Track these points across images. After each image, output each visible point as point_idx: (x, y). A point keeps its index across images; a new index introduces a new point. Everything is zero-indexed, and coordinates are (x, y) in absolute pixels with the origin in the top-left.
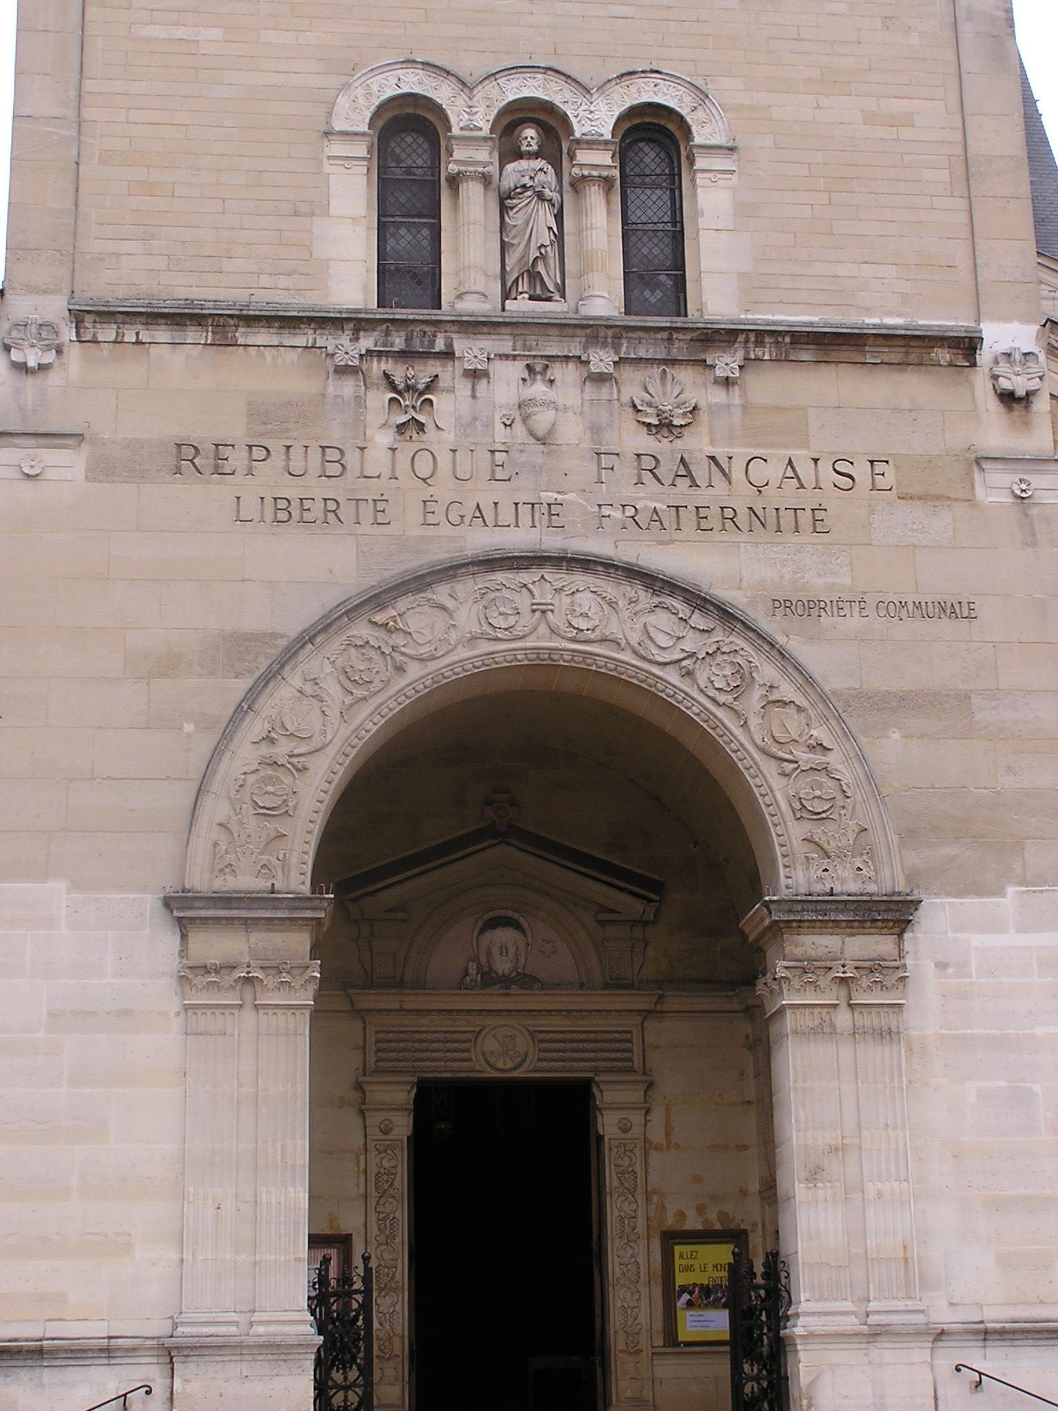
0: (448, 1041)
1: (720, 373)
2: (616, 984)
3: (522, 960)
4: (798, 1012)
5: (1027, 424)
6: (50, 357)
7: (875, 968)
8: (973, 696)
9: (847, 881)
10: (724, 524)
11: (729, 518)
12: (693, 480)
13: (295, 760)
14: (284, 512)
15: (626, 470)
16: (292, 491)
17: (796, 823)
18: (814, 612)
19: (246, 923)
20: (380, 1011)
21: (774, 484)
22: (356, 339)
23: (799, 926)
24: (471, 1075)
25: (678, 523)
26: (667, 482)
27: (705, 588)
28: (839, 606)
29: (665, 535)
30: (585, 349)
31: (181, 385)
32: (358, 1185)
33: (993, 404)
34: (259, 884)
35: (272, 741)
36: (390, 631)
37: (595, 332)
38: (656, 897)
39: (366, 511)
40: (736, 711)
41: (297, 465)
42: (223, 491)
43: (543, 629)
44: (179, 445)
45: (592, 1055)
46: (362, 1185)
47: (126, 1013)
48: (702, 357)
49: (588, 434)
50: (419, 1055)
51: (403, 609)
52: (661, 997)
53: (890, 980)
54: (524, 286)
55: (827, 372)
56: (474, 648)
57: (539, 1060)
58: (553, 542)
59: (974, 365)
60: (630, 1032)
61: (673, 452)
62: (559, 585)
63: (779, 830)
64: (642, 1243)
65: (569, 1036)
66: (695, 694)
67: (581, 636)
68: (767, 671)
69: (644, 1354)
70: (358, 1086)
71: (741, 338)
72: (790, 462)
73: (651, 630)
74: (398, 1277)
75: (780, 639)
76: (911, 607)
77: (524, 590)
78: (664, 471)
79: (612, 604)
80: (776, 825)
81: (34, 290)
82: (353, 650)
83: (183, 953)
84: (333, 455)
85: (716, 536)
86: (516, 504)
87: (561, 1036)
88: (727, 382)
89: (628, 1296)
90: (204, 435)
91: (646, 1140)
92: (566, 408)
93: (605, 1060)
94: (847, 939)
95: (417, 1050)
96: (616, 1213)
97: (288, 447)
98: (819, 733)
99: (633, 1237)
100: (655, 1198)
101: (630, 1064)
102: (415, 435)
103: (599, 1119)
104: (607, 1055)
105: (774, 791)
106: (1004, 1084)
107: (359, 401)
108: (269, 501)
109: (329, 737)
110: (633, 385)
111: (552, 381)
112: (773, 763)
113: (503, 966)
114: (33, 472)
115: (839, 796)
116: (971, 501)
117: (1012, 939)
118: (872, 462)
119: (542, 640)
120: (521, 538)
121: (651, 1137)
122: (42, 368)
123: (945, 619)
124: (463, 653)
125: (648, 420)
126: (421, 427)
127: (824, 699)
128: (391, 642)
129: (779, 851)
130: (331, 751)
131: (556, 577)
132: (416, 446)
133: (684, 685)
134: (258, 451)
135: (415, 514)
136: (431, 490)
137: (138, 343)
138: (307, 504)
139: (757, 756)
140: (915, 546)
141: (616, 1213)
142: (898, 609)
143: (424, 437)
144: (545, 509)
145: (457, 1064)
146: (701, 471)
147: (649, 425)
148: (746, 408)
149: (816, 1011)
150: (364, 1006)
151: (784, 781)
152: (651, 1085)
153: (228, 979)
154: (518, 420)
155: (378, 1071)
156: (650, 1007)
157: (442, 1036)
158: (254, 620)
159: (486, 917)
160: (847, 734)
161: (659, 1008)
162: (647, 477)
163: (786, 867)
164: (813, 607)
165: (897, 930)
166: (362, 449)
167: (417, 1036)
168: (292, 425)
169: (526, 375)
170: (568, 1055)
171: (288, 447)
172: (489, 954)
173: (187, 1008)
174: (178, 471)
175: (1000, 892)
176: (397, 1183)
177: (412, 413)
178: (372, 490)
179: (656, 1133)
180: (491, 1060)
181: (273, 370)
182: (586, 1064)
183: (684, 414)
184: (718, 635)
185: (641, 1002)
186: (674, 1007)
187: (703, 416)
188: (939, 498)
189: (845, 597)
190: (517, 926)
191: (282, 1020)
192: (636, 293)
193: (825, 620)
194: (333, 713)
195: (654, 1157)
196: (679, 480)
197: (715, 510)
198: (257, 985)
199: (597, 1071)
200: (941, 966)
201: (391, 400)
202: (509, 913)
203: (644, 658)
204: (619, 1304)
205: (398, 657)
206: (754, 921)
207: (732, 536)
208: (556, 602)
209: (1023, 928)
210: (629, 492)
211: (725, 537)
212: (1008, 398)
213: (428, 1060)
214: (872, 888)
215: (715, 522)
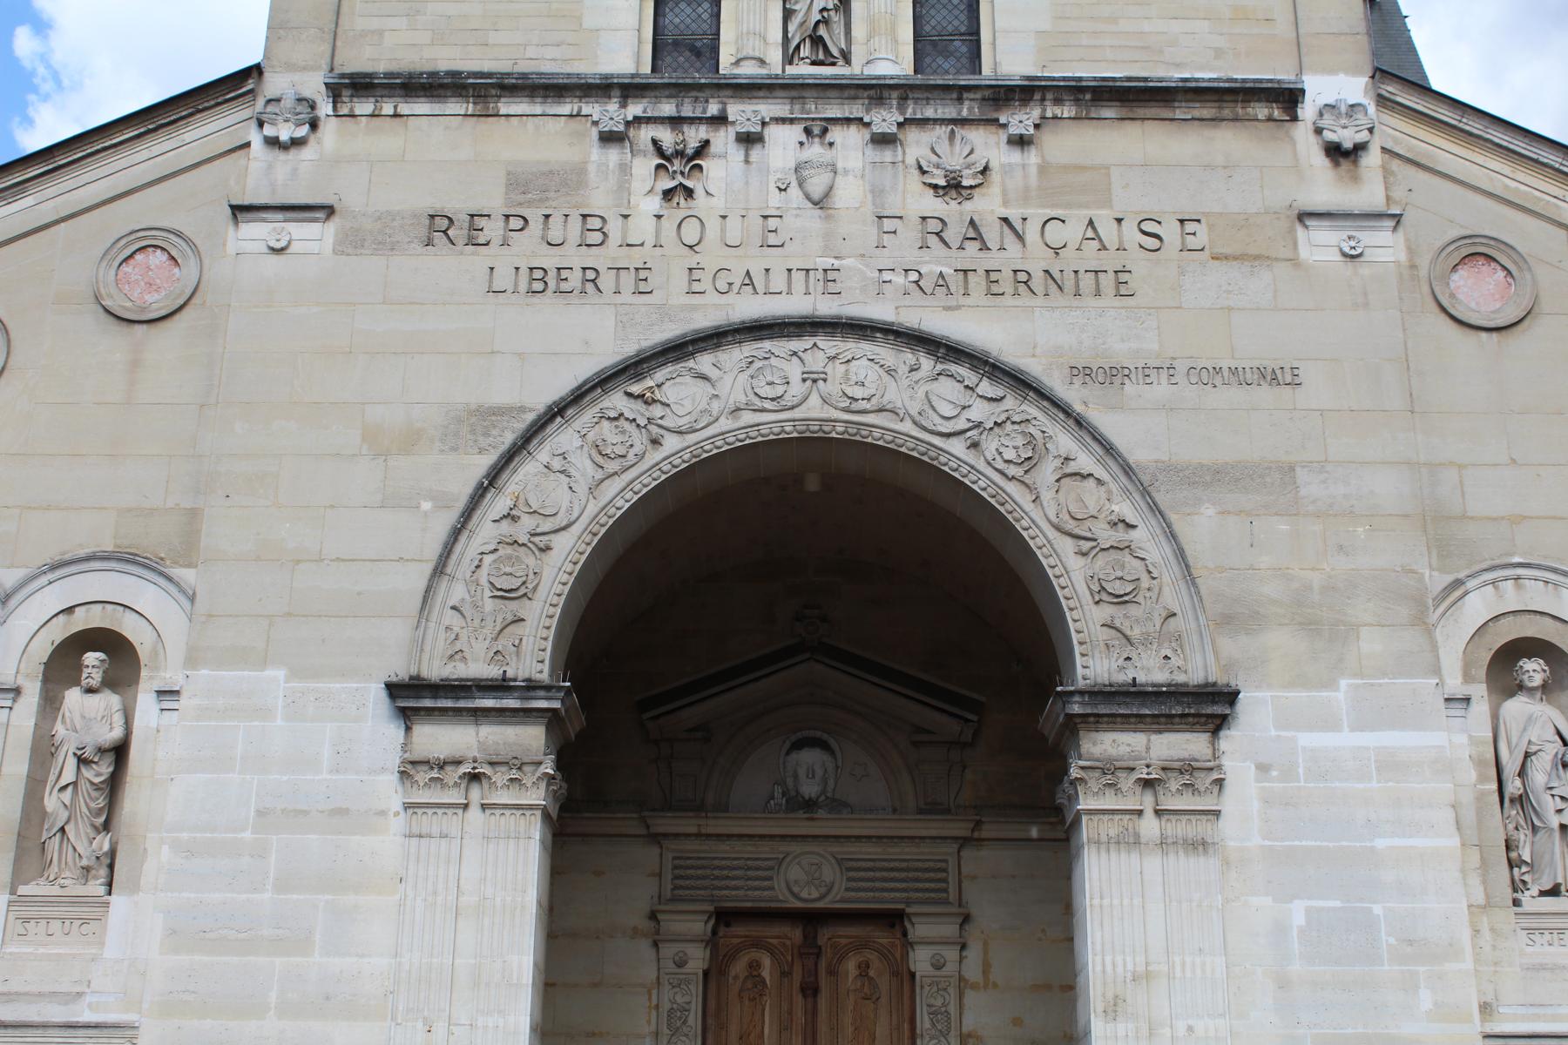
0: (749, 869)
1: (1015, 130)
2: (931, 809)
3: (831, 783)
4: (1095, 818)
5: (1355, 179)
6: (303, 131)
7: (1188, 768)
8: (1298, 469)
9: (1151, 670)
10: (1016, 289)
11: (1023, 281)
12: (983, 241)
13: (536, 539)
14: (539, 282)
15: (909, 234)
16: (550, 260)
17: (1094, 608)
18: (1117, 380)
19: (479, 715)
20: (677, 835)
21: (1072, 246)
22: (623, 105)
23: (1097, 722)
24: (773, 905)
25: (966, 288)
26: (955, 244)
27: (994, 353)
28: (1146, 373)
29: (952, 302)
30: (868, 111)
31: (441, 155)
32: (649, 1022)
33: (1320, 160)
34: (493, 672)
35: (515, 519)
36: (646, 403)
37: (876, 91)
38: (975, 718)
39: (627, 280)
40: (1027, 486)
41: (555, 234)
42: (475, 262)
43: (814, 400)
44: (432, 217)
45: (904, 885)
46: (654, 1021)
47: (341, 812)
48: (995, 115)
49: (870, 197)
50: (716, 882)
51: (661, 380)
52: (978, 824)
53: (1204, 781)
54: (806, 51)
55: (1133, 130)
56: (737, 419)
57: (847, 889)
58: (827, 307)
59: (1295, 119)
60: (946, 861)
61: (961, 214)
62: (832, 352)
63: (1076, 615)
65: (878, 864)
66: (982, 466)
67: (855, 406)
68: (1064, 441)
70: (653, 916)
71: (1037, 96)
72: (1091, 223)
73: (934, 399)
75: (1078, 408)
76: (1226, 374)
77: (795, 359)
78: (952, 235)
79: (890, 372)
80: (1071, 609)
81: (290, 67)
82: (605, 423)
83: (405, 747)
84: (595, 223)
85: (1008, 300)
86: (789, 270)
87: (870, 864)
88: (1021, 142)
90: (458, 204)
91: (961, 978)
92: (846, 172)
93: (917, 890)
94: (1154, 737)
95: (717, 878)
97: (547, 217)
98: (1124, 509)
102: (682, 201)
104: (920, 885)
105: (1070, 572)
106: (1338, 904)
107: (625, 169)
108: (524, 272)
109: (575, 515)
110: (917, 145)
111: (831, 144)
112: (1069, 541)
113: (810, 789)
114: (278, 245)
115: (1145, 577)
116: (1294, 261)
117: (1346, 739)
118: (1182, 221)
119: (814, 409)
120: (795, 305)
121: (967, 974)
122: (297, 143)
123: (1265, 386)
124: (725, 424)
125: (934, 181)
126: (689, 193)
127: (1128, 470)
128: (648, 414)
129: (1075, 637)
130: (576, 529)
131: (829, 345)
132: (682, 213)
133: (969, 457)
134: (516, 221)
135: (680, 281)
136: (697, 258)
137: (396, 115)
138: (564, 274)
139: (1052, 533)
140: (1230, 309)
142: (1210, 376)
143: (691, 203)
144: (820, 275)
145: (757, 893)
146: (992, 233)
147: (935, 187)
148: (1043, 169)
149: (1117, 817)
150: (661, 830)
151: (1081, 561)
152: (967, 919)
153: (452, 775)
154: (794, 184)
155: (673, 900)
156: (967, 833)
157: (741, 863)
158: (502, 393)
159: (793, 738)
160: (1155, 509)
161: (976, 835)
162: (933, 241)
163: (1083, 655)
164: (1115, 375)
165: (1211, 726)
166: (626, 217)
167: (716, 862)
168: (552, 194)
169: (803, 138)
170: (878, 884)
171: (547, 217)
172: (796, 776)
173: (408, 806)
174: (429, 243)
175: (1331, 684)
176: (691, 1021)
177: (680, 179)
178: (635, 258)
179: (972, 971)
180: (796, 889)
181: (537, 138)
183: (974, 175)
184: (1010, 402)
185: (959, 829)
186: (993, 835)
187: (995, 176)
188: (1257, 257)
189: (1152, 363)
190: (824, 746)
191: (510, 821)
192: (928, 60)
193: (1129, 388)
194: (582, 489)
195: (970, 997)
196: (968, 244)
197: (1007, 274)
198: (484, 781)
199: (909, 902)
200: (1263, 768)
201: (659, 167)
202: (818, 734)
203: (925, 429)
205: (654, 429)
206: (1050, 719)
207: (1026, 299)
208: (829, 369)
209: (1358, 727)
210: (912, 256)
211: (1018, 301)
212: (1335, 152)
213: (727, 888)
214: (1180, 678)
215: (1006, 285)
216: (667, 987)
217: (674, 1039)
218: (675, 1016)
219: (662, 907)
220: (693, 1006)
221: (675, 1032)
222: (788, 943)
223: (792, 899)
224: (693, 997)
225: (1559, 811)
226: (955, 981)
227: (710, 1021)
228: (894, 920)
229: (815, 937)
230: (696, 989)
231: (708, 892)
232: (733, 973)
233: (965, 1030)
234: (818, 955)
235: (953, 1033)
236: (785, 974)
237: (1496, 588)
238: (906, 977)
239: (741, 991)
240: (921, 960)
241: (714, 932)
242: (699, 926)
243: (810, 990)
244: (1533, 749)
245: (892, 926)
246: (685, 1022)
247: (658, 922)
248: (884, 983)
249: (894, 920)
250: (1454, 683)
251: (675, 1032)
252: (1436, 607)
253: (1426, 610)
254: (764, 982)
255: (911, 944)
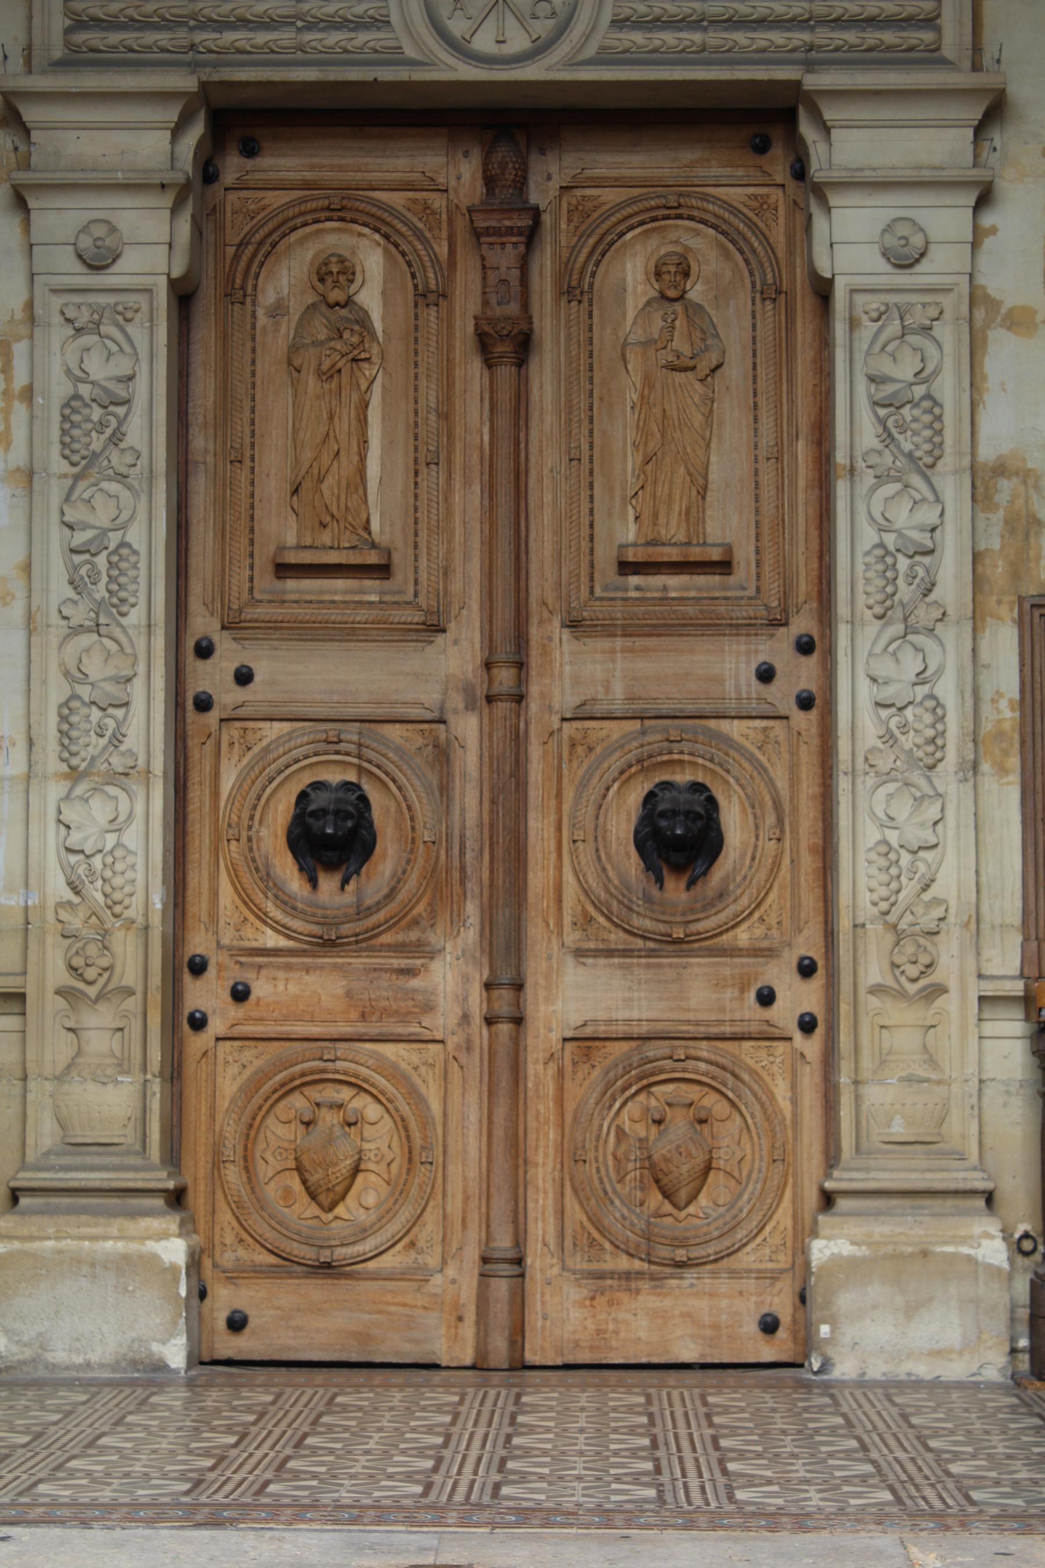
24: (386, 74)
64: (954, 638)
69: (949, 1003)
74: (134, 740)
89: (902, 810)
96: (869, 536)
99: (924, 615)
100: (1005, 487)
101: (928, 36)
103: (819, 223)
141: (869, 536)
145: (334, 38)
152: (995, 111)
155: (73, 61)
176: (135, 434)
180: (458, 27)
182: (777, 37)
195: (1003, 351)
204: (871, 835)
216: (59, 333)
217: (83, 489)
218: (85, 427)
219: (38, 82)
220: (141, 385)
221: (85, 466)
222: (438, 202)
223: (445, 56)
224: (139, 358)
226: (955, 304)
227: (199, 441)
228: (764, 121)
229: (521, 184)
230: (151, 336)
231: (182, 37)
232: (268, 297)
233: (986, 453)
234: (531, 235)
235: (948, 462)
236: (429, 297)
238: (804, 303)
239: (294, 349)
240: (849, 241)
241: (208, 172)
242: (153, 143)
243: (507, 344)
245: (762, 147)
246: (116, 438)
247: (27, 132)
248: (735, 323)
249: (764, 121)
251: (85, 466)
254: (363, 321)
255: (819, 191)
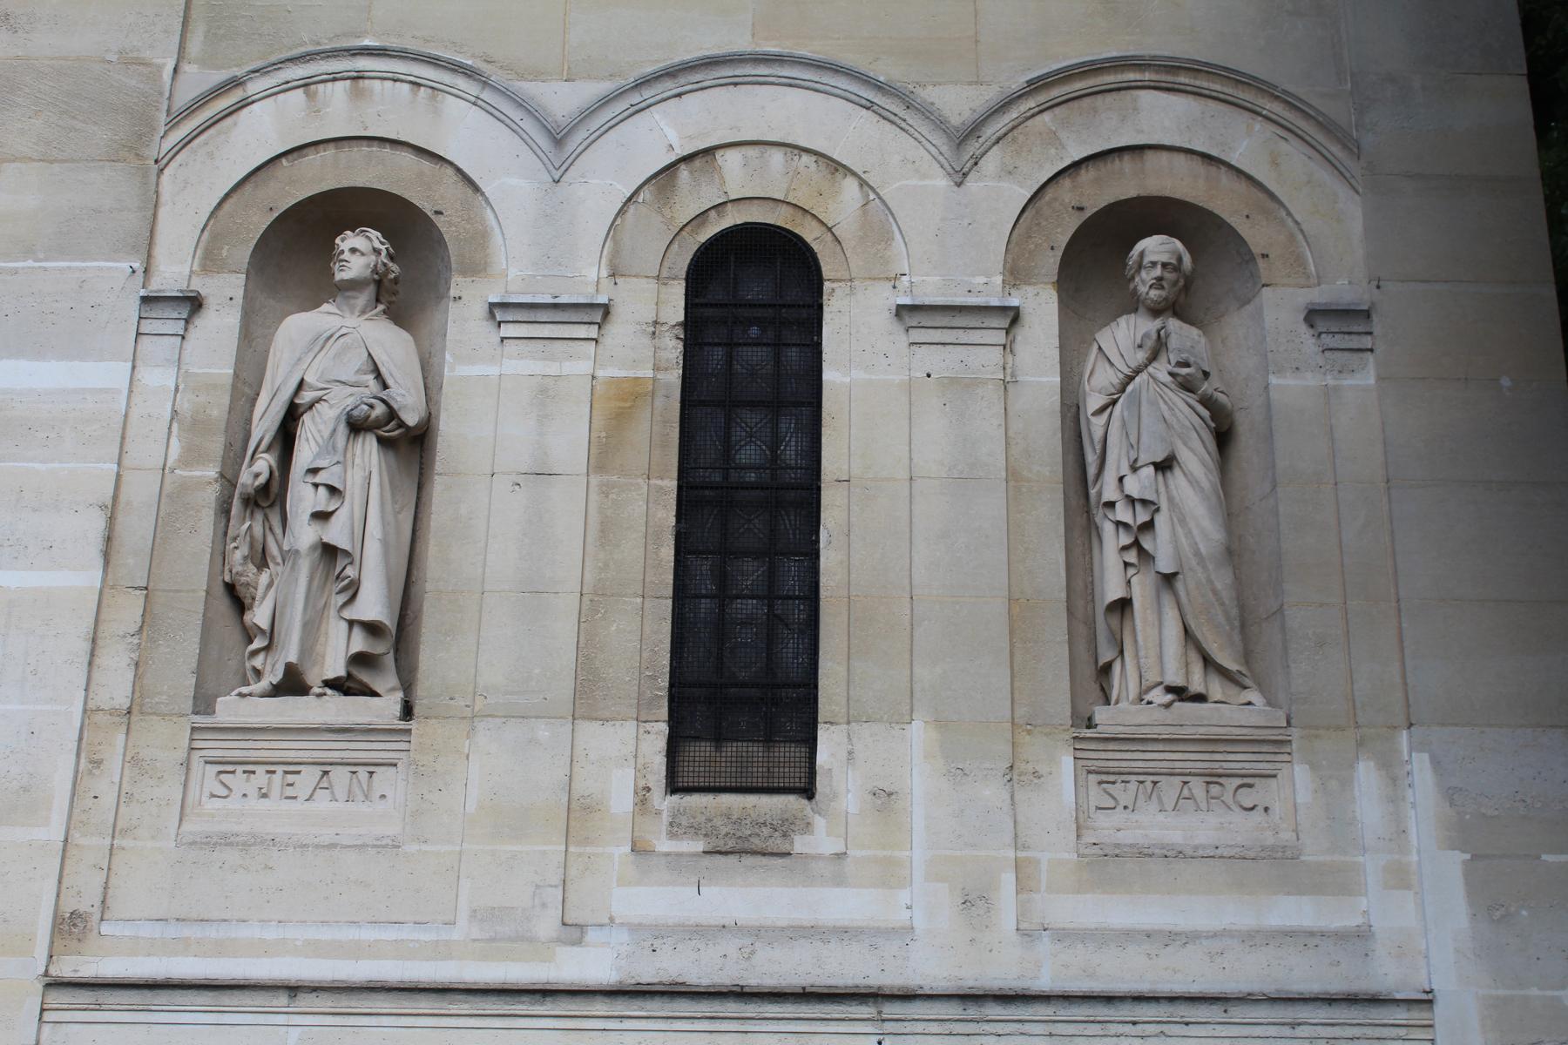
225: (322, 516)
237: (310, 96)
244: (306, 397)
250: (172, 274)
252: (173, 124)
253: (151, 131)
